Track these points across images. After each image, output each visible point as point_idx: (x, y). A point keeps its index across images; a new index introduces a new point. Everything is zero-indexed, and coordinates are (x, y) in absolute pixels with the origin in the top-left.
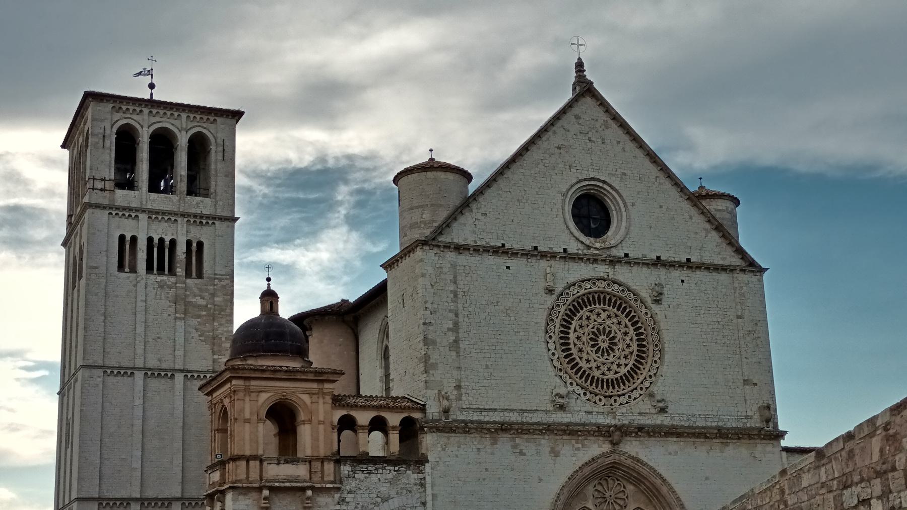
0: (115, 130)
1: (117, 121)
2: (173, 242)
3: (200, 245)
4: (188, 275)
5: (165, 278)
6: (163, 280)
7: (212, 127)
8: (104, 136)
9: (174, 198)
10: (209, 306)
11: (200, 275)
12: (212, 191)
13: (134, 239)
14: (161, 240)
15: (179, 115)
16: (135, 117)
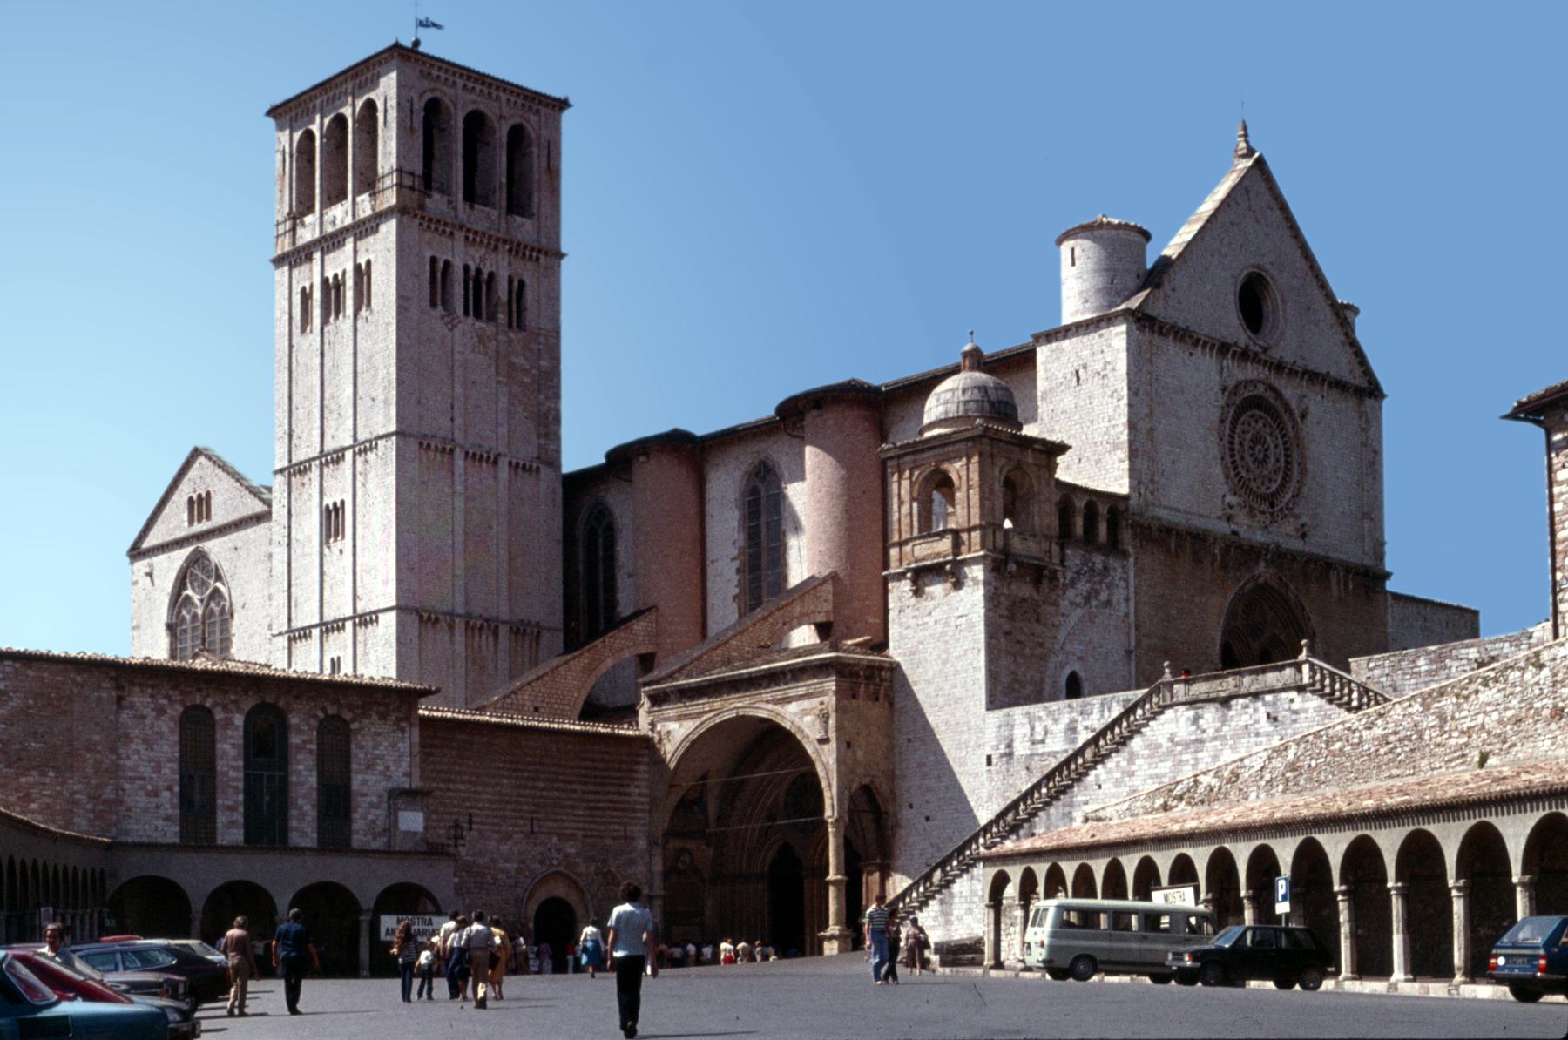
0: (423, 105)
1: (425, 92)
2: (491, 275)
3: (522, 284)
4: (510, 325)
5: (483, 325)
6: (480, 328)
7: (533, 118)
8: (412, 111)
9: (494, 213)
10: (534, 371)
11: (521, 326)
12: (535, 211)
13: (447, 264)
14: (479, 271)
15: (497, 97)
16: (450, 91)
